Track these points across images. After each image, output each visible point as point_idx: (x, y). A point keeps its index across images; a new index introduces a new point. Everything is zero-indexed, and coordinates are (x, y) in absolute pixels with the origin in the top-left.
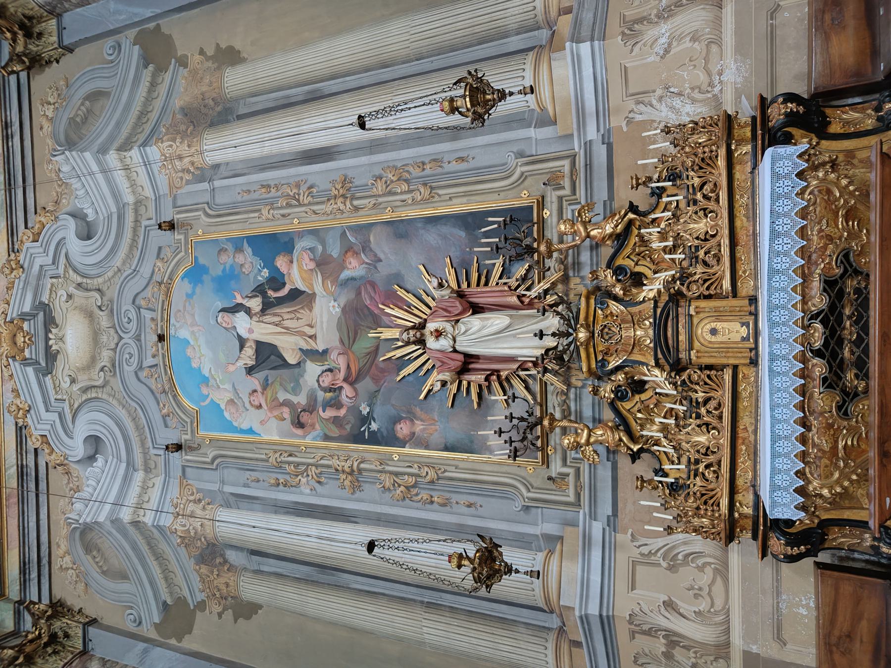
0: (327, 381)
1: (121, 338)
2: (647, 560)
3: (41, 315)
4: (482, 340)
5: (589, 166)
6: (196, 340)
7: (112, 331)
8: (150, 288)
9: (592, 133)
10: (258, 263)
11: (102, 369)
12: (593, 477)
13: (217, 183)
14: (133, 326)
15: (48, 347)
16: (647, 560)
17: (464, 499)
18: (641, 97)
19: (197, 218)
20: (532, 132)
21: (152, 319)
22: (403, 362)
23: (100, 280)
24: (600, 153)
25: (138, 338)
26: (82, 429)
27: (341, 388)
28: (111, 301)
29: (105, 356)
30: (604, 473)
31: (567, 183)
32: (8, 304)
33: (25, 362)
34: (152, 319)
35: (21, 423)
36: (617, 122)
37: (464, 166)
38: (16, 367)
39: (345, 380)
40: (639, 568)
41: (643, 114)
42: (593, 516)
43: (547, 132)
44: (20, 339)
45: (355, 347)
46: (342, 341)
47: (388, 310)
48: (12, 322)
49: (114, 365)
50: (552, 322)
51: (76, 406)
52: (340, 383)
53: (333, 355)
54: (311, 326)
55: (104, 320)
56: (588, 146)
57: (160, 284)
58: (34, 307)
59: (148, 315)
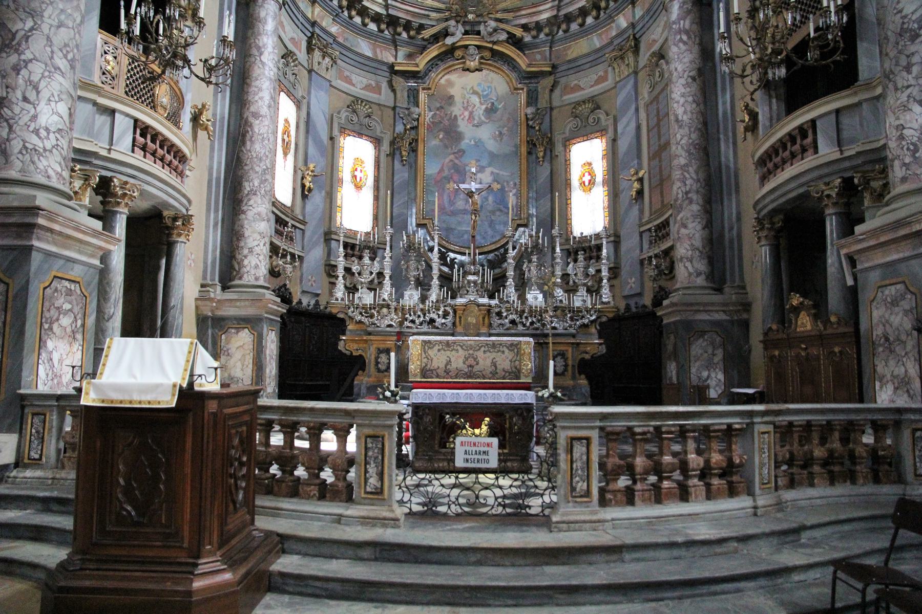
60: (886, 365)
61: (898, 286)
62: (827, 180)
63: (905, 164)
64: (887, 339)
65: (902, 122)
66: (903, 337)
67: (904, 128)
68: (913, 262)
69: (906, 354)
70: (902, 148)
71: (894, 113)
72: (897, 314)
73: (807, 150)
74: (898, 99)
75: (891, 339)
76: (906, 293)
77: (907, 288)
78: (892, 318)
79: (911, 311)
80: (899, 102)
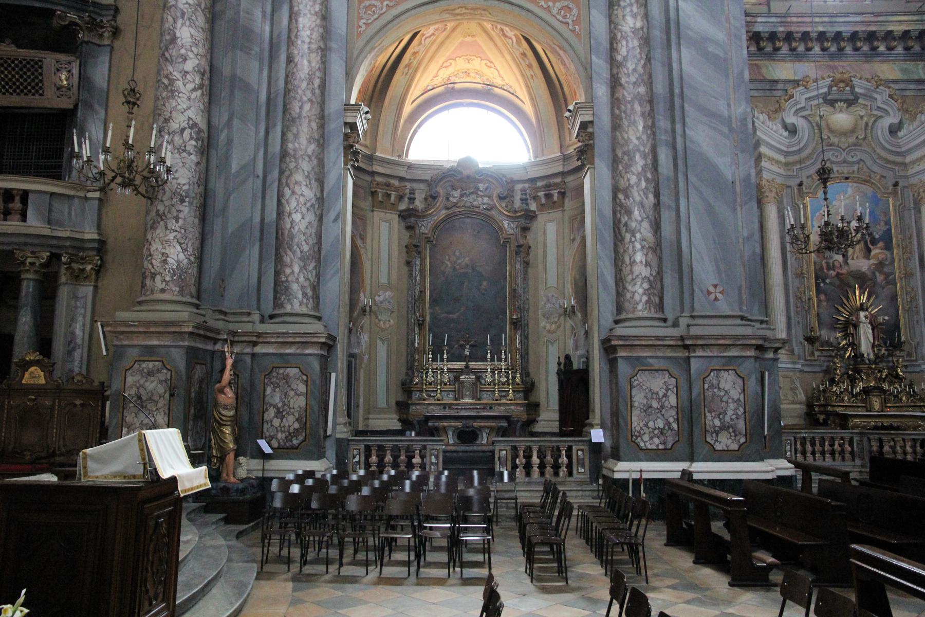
0: (837, 264)
1: (844, 150)
2: (792, 382)
3: (852, 97)
4: (865, 333)
6: (847, 198)
7: (847, 145)
8: (868, 171)
10: (881, 233)
11: (829, 137)
12: (816, 365)
13: (913, 211)
14: (850, 159)
15: (836, 101)
16: (792, 382)
17: (800, 319)
19: (899, 201)
21: (854, 171)
22: (848, 299)
23: (870, 138)
25: (845, 162)
26: (800, 123)
27: (834, 270)
28: (860, 146)
29: (835, 140)
30: (818, 369)
31: (908, 358)
33: (830, 87)
34: (854, 171)
35: (801, 83)
38: (828, 81)
39: (838, 273)
40: (789, 379)
42: (803, 365)
44: (842, 85)
45: (850, 278)
46: (852, 271)
47: (866, 294)
48: (851, 81)
49: (831, 145)
50: (872, 357)
51: (810, 119)
52: (836, 270)
53: (846, 268)
54: (857, 258)
55: (852, 140)
57: (870, 177)
58: (857, 93)
59: (855, 168)
60: (136, 416)
61: (157, 363)
62: (34, 249)
63: (165, 281)
64: (139, 398)
65: (167, 252)
66: (156, 398)
67: (168, 257)
68: (172, 350)
69: (157, 409)
70: (165, 269)
71: (162, 244)
72: (153, 381)
73: (10, 213)
74: (166, 236)
75: (144, 398)
76: (162, 369)
77: (164, 366)
78: (147, 384)
79: (166, 381)
80: (167, 238)
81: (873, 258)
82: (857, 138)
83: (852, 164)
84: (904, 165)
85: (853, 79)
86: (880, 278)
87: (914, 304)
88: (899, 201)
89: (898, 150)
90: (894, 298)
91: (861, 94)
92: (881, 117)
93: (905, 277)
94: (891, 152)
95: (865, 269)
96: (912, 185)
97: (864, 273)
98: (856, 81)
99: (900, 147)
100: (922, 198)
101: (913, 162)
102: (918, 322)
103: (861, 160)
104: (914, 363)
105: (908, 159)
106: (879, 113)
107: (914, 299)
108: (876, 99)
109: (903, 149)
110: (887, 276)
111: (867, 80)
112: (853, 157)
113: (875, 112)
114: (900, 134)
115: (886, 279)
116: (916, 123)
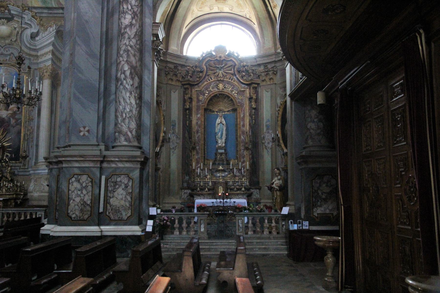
1: (2, 47)
3: (11, 17)
5: (25, 171)
7: (4, 44)
9: (31, 172)
14: (5, 53)
18: (36, 181)
20: (34, 161)
23: (19, 41)
24: (28, 174)
28: (13, 45)
32: (13, 6)
34: (7, 60)
36: (32, 177)
37: (30, 147)
41: (33, 181)
43: (33, 164)
56: (29, 171)
59: (8, 58)
81: (10, 110)
82: (11, 40)
83: (6, 55)
84: (37, 56)
85: (8, 5)
86: (13, 121)
87: (31, 137)
88: (31, 77)
89: (35, 48)
90: (19, 133)
91: (15, 15)
92: (27, 28)
93: (28, 121)
94: (30, 49)
95: (4, 116)
96: (40, 68)
97: (4, 119)
98: (11, 7)
99: (35, 46)
100: (44, 76)
101: (42, 55)
102: (32, 146)
103: (12, 53)
104: (26, 170)
105: (39, 54)
106: (26, 26)
107: (32, 133)
108: (24, 18)
109: (38, 47)
110: (17, 120)
111: (18, 7)
112: (7, 51)
113: (23, 26)
114: (37, 38)
115: (15, 122)
116: (47, 33)
